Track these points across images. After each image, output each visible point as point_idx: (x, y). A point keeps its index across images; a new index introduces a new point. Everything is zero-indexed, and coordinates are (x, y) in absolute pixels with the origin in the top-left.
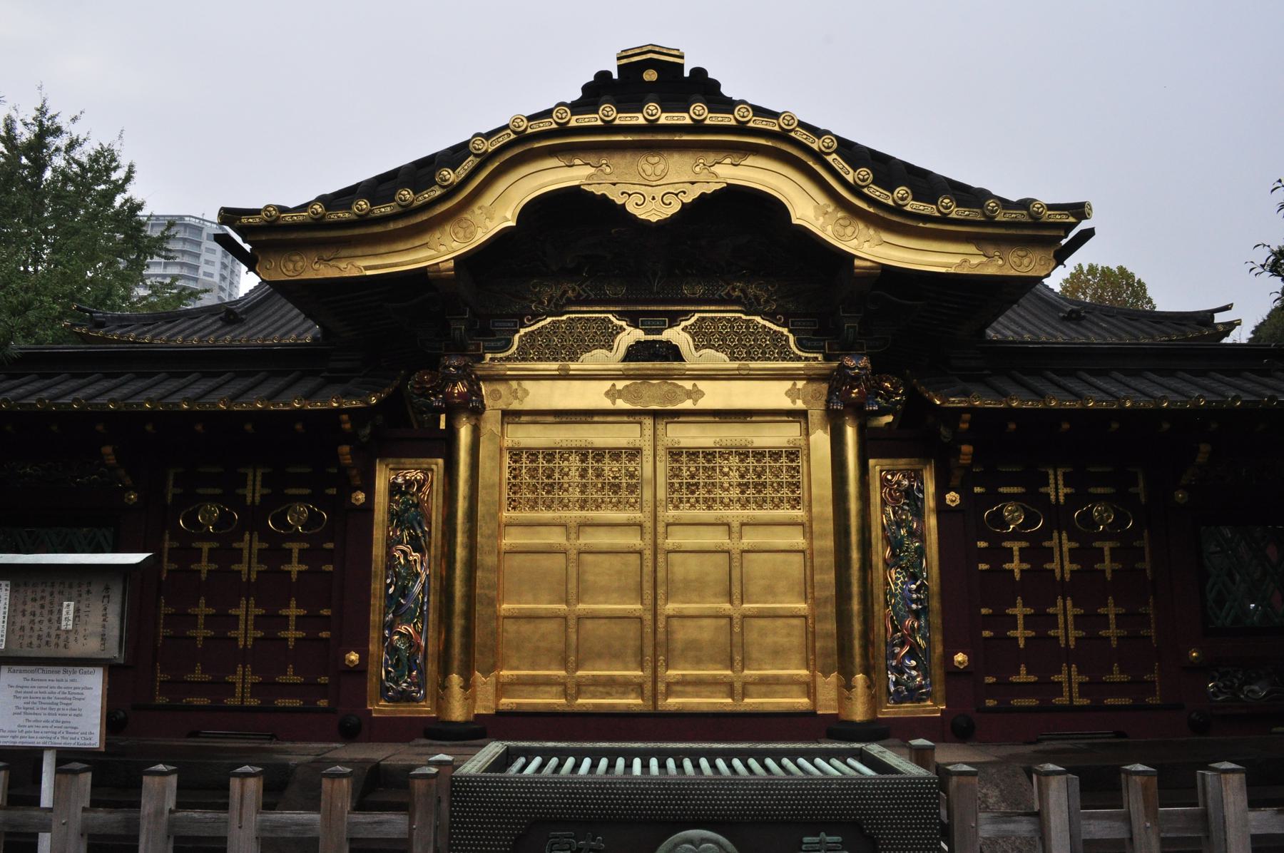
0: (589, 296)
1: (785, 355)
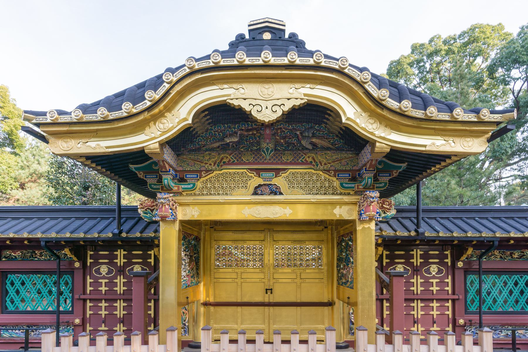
0: (234, 161)
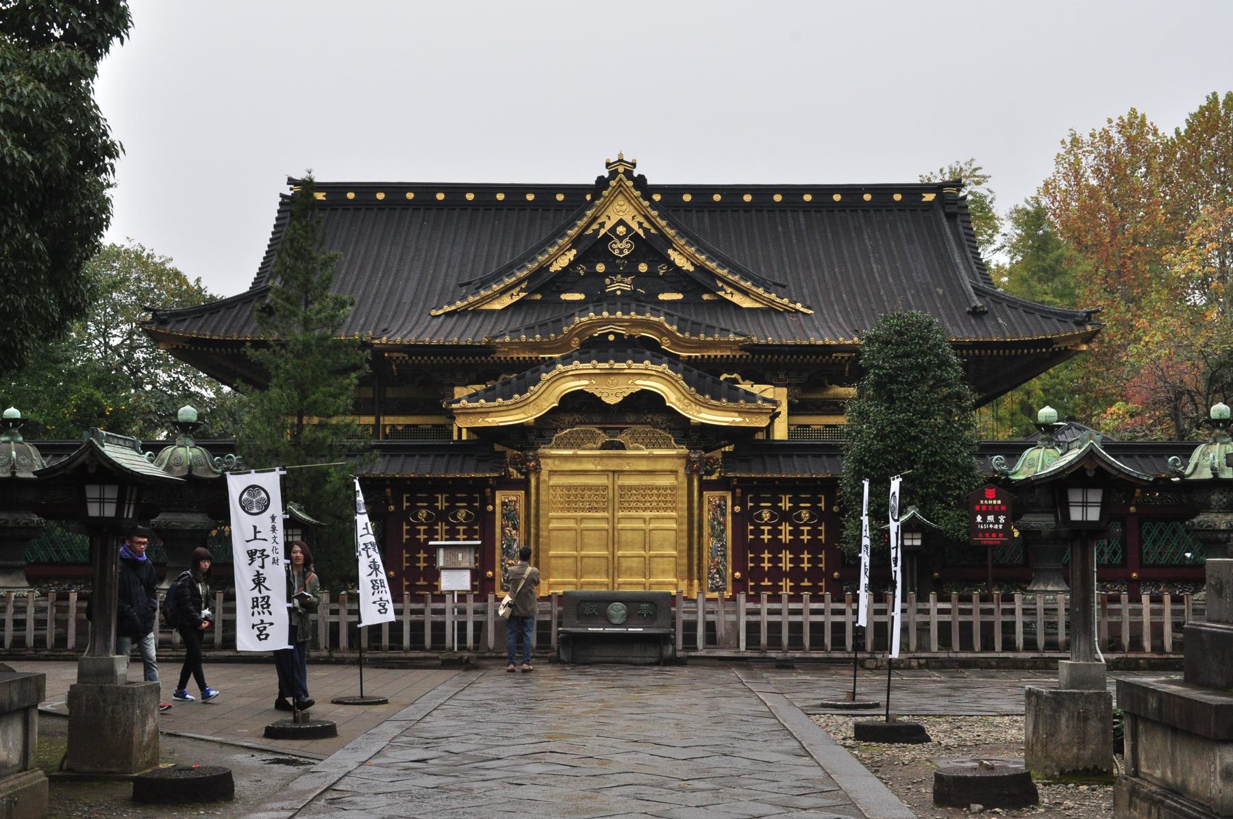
1: (669, 447)
